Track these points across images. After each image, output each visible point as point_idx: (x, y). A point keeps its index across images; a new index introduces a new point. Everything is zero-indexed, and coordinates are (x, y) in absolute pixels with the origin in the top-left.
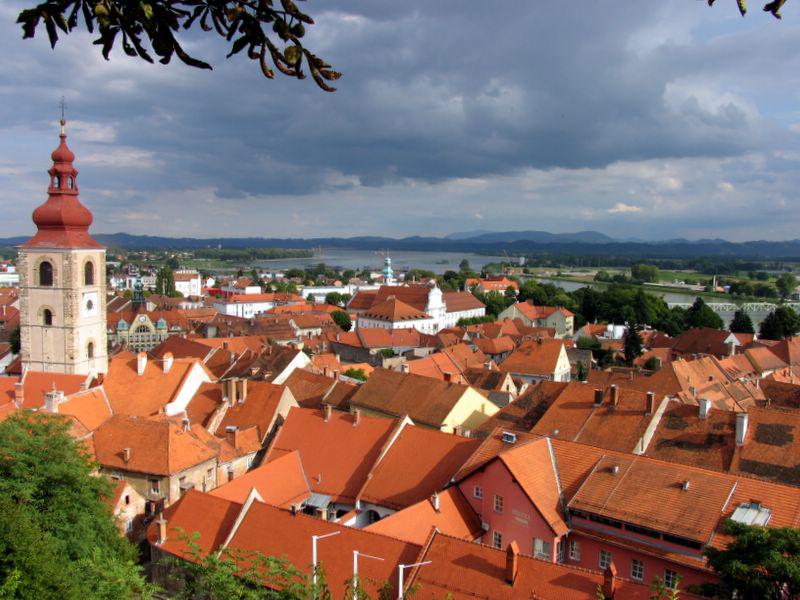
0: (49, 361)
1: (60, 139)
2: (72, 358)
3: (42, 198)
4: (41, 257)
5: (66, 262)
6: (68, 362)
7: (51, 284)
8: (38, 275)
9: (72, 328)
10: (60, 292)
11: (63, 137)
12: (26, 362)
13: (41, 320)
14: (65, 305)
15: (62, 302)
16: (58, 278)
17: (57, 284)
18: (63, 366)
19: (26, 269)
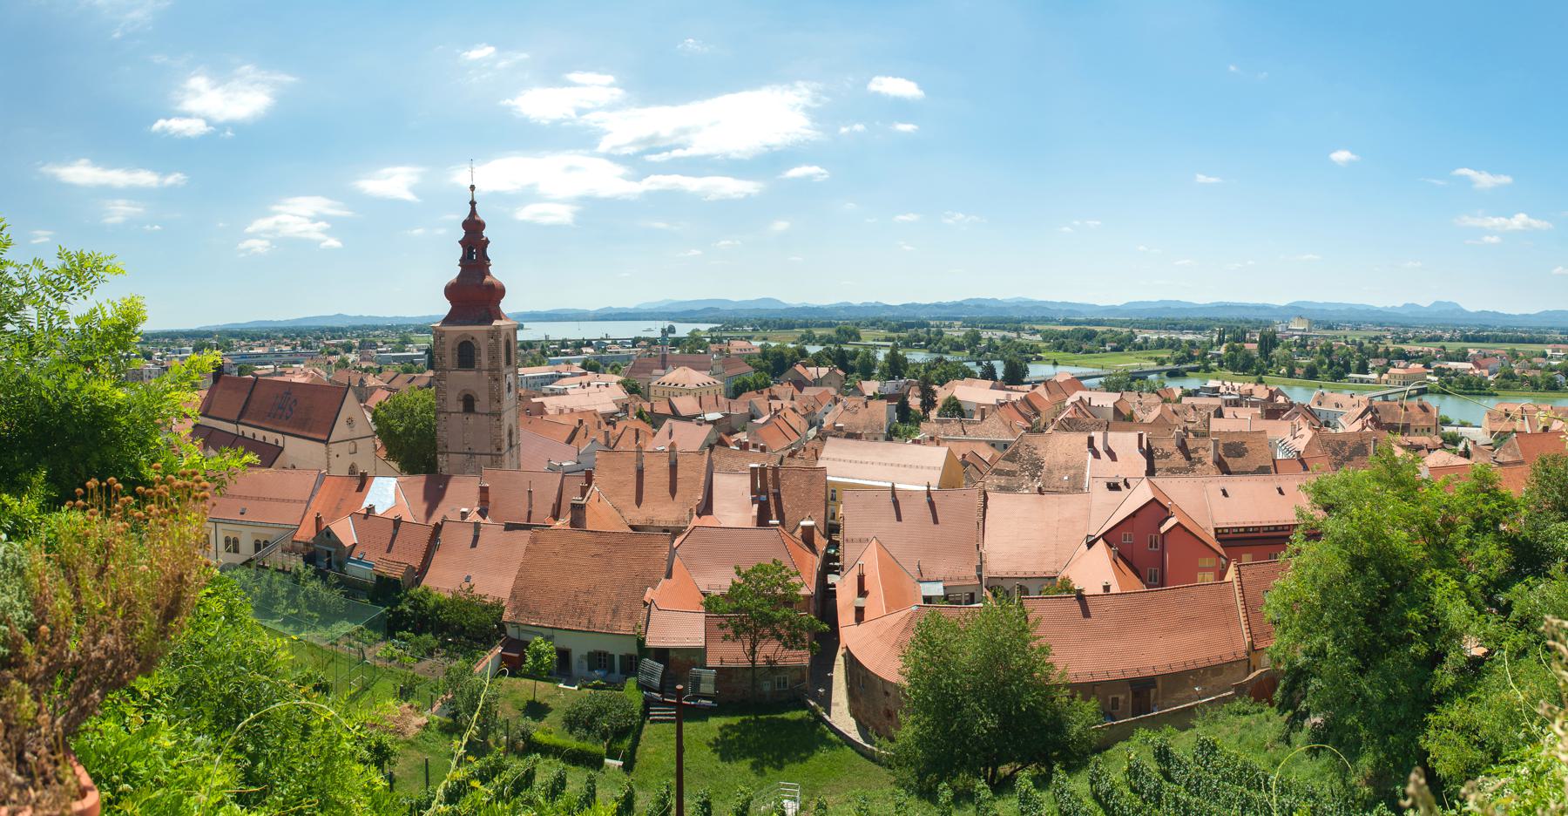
0: (472, 451)
1: (470, 206)
2: (499, 449)
3: (453, 272)
5: (492, 341)
6: (494, 452)
9: (500, 415)
11: (473, 203)
12: (442, 453)
13: (461, 407)
14: (491, 388)
15: (487, 385)
16: (484, 360)
17: (480, 363)
19: (444, 349)
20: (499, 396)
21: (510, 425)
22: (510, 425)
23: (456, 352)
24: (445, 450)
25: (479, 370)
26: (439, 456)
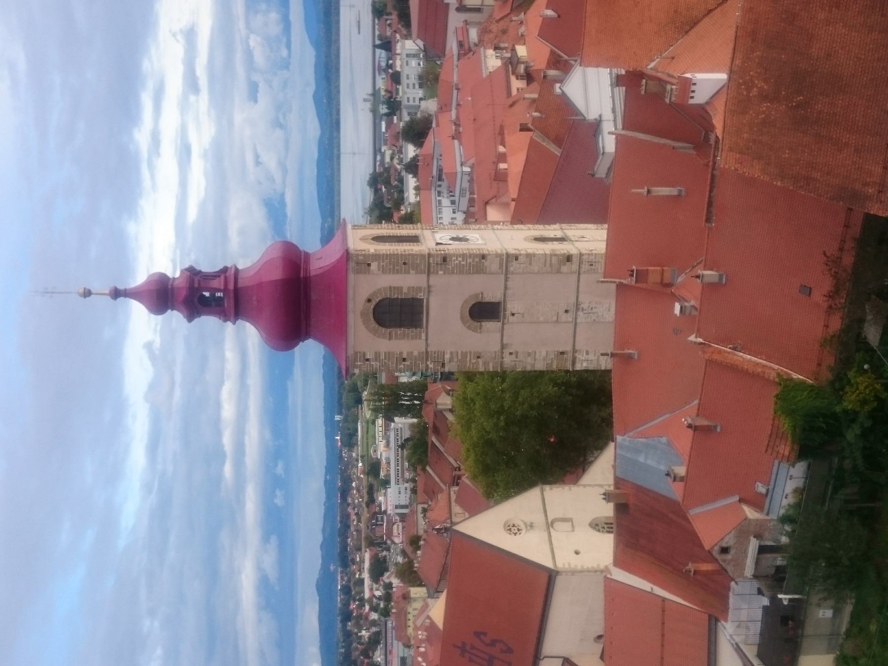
2: (569, 258)
4: (366, 322)
5: (374, 266)
7: (423, 299)
8: (399, 331)
9: (508, 255)
10: (434, 280)
14: (461, 270)
17: (419, 289)
18: (583, 277)
19: (388, 355)
20: (476, 256)
21: (525, 239)
22: (525, 239)
24: (569, 356)
26: (578, 367)
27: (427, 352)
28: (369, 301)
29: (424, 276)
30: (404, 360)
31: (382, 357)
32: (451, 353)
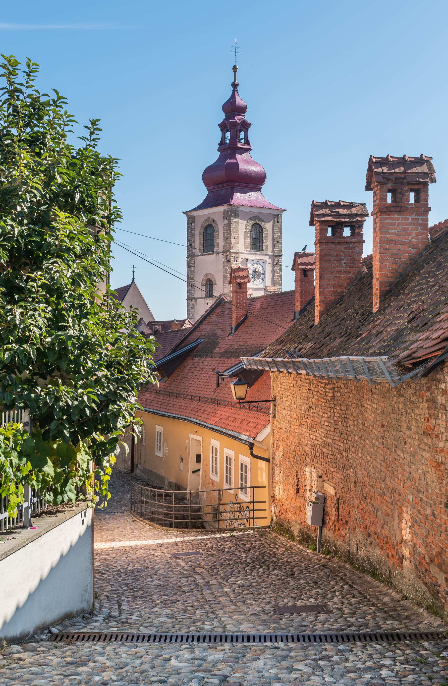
1: (232, 88)
5: (226, 221)
10: (221, 256)
11: (235, 86)
15: (222, 267)
23: (202, 237)
25: (217, 253)
27: (194, 256)
28: (214, 221)
29: (222, 250)
30: (191, 245)
31: (192, 232)
32: (194, 271)
